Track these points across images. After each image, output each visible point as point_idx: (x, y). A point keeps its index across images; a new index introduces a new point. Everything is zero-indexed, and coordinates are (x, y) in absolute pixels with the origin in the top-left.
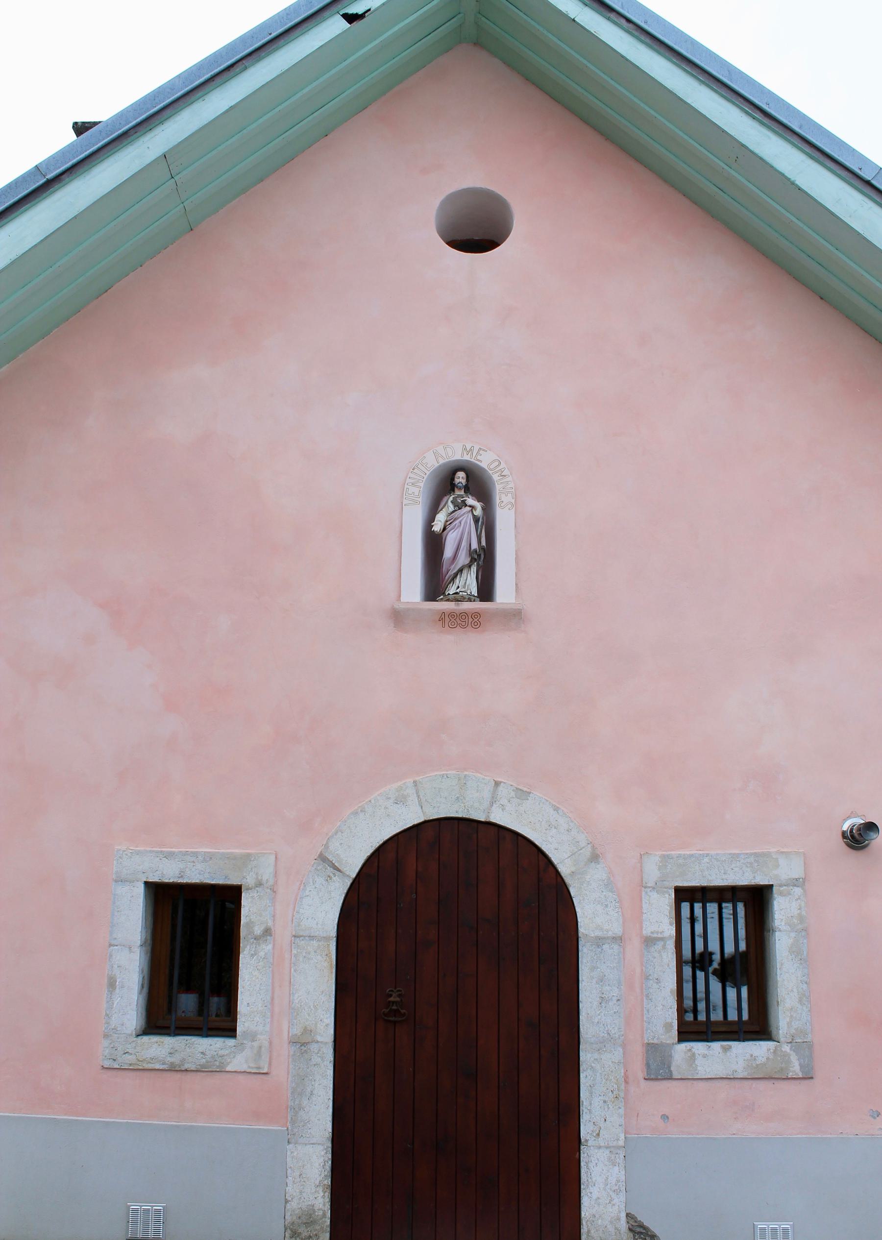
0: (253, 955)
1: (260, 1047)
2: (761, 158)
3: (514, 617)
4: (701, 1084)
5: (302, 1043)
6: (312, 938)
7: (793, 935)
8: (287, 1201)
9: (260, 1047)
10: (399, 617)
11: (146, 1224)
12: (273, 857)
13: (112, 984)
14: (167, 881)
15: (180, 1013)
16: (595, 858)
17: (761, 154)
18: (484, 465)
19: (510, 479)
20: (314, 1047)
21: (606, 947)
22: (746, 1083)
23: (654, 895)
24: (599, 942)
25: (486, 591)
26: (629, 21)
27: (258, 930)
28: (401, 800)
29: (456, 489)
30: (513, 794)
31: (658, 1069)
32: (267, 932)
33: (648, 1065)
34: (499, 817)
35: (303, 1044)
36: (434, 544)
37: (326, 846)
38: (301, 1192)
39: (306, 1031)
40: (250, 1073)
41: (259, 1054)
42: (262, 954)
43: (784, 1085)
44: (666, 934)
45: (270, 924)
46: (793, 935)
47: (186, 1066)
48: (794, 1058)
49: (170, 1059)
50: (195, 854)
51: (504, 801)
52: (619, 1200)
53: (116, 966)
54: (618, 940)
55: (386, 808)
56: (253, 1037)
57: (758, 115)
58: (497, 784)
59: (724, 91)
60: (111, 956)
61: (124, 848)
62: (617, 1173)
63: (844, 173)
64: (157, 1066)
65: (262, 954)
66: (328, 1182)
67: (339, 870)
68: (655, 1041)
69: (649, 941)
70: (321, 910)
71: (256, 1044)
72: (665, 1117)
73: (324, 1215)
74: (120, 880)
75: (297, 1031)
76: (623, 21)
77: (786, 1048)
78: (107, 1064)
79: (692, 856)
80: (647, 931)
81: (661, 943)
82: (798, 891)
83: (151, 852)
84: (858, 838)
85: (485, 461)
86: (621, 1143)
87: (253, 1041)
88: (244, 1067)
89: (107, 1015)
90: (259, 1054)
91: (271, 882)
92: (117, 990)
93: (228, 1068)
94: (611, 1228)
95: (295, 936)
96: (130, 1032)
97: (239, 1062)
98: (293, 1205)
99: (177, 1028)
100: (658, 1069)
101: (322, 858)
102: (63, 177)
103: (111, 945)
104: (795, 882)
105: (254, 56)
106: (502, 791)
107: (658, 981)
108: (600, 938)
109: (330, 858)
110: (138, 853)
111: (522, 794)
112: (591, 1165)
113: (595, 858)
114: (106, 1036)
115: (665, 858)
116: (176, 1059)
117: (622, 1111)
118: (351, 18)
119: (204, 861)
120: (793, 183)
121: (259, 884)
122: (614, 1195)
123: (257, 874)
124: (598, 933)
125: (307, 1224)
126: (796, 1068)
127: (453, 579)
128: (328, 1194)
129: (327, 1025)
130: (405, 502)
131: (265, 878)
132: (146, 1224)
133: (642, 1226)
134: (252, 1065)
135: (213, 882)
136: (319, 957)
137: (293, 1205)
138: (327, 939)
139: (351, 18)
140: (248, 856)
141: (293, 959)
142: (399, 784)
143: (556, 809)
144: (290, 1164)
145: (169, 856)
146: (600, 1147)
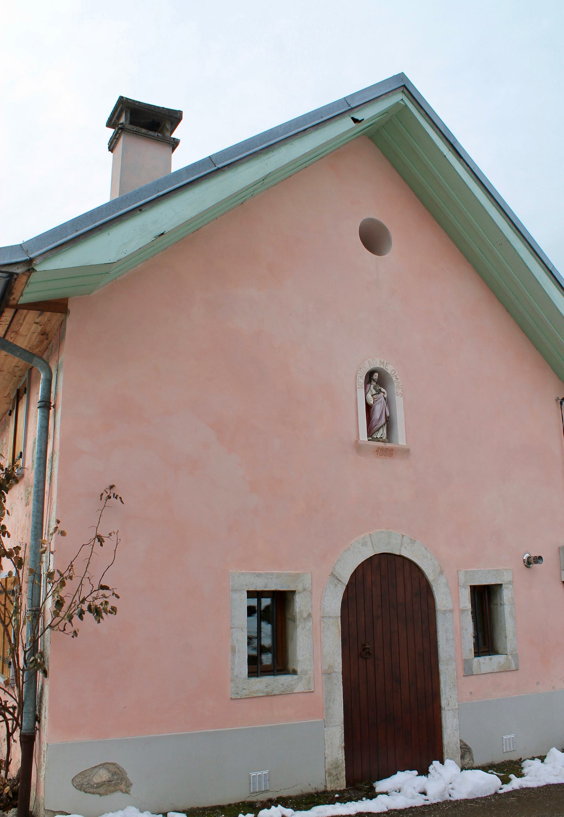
0: (303, 629)
1: (310, 678)
2: (514, 249)
3: (406, 452)
4: (483, 676)
5: (328, 673)
6: (330, 617)
7: (510, 606)
8: (325, 758)
9: (310, 678)
10: (358, 447)
11: (260, 783)
12: (310, 575)
13: (233, 650)
14: (258, 590)
15: (263, 664)
16: (441, 572)
17: (515, 247)
18: (389, 371)
19: (399, 381)
20: (334, 675)
21: (447, 615)
22: (498, 674)
23: (463, 589)
24: (445, 612)
25: (389, 437)
26: (468, 165)
27: (305, 615)
28: (364, 544)
29: (372, 381)
30: (409, 541)
31: (468, 672)
32: (310, 615)
33: (464, 669)
34: (405, 553)
35: (329, 674)
36: (369, 408)
37: (334, 568)
38: (332, 752)
39: (330, 667)
40: (306, 692)
41: (309, 682)
42: (307, 628)
43: (509, 674)
44: (468, 608)
45: (310, 611)
46: (510, 606)
47: (275, 692)
48: (513, 661)
49: (266, 690)
50: (272, 574)
51: (406, 545)
52: (457, 734)
53: (235, 640)
54: (451, 611)
55: (358, 548)
56: (305, 672)
57: (514, 228)
58: (403, 536)
59: (502, 212)
60: (232, 634)
61: (234, 571)
62: (456, 721)
63: (541, 263)
64: (260, 695)
65: (307, 628)
66: (343, 745)
67: (340, 581)
68: (467, 658)
69: (462, 611)
70: (333, 603)
71: (307, 676)
72: (471, 693)
73: (343, 762)
74: (234, 590)
75: (325, 667)
76: (465, 165)
77: (510, 657)
78: (233, 697)
79: (475, 571)
80: (461, 607)
81: (466, 612)
82: (511, 586)
83: (249, 573)
84: (530, 562)
85: (389, 369)
86: (457, 707)
87: (306, 675)
88: (303, 690)
89: (232, 668)
90: (309, 682)
91: (310, 588)
92: (237, 654)
93: (295, 692)
94: (455, 748)
95: (322, 617)
96: (244, 677)
97: (300, 688)
98: (329, 760)
99: (277, 671)
100: (468, 672)
101: (332, 575)
102: (225, 168)
103: (231, 628)
104: (510, 583)
105: (315, 127)
106: (406, 540)
107: (466, 630)
108: (445, 611)
109: (336, 574)
110: (243, 574)
111: (413, 541)
112: (447, 719)
113: (441, 572)
114: (232, 681)
115: (466, 572)
116: (269, 690)
117: (456, 692)
118: (355, 121)
119: (277, 578)
120: (525, 264)
121: (305, 590)
122: (455, 732)
123: (303, 584)
124: (444, 609)
125: (335, 768)
126: (513, 667)
127: (378, 430)
128: (343, 751)
129: (339, 663)
130: (358, 386)
131: (307, 587)
132: (260, 783)
133: (465, 745)
134: (307, 688)
135: (282, 590)
136: (334, 627)
137: (329, 760)
138: (336, 617)
139: (355, 121)
140: (299, 574)
141: (322, 628)
142: (363, 535)
143: (426, 549)
144: (326, 739)
145: (259, 575)
146: (449, 710)
